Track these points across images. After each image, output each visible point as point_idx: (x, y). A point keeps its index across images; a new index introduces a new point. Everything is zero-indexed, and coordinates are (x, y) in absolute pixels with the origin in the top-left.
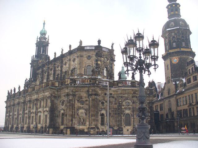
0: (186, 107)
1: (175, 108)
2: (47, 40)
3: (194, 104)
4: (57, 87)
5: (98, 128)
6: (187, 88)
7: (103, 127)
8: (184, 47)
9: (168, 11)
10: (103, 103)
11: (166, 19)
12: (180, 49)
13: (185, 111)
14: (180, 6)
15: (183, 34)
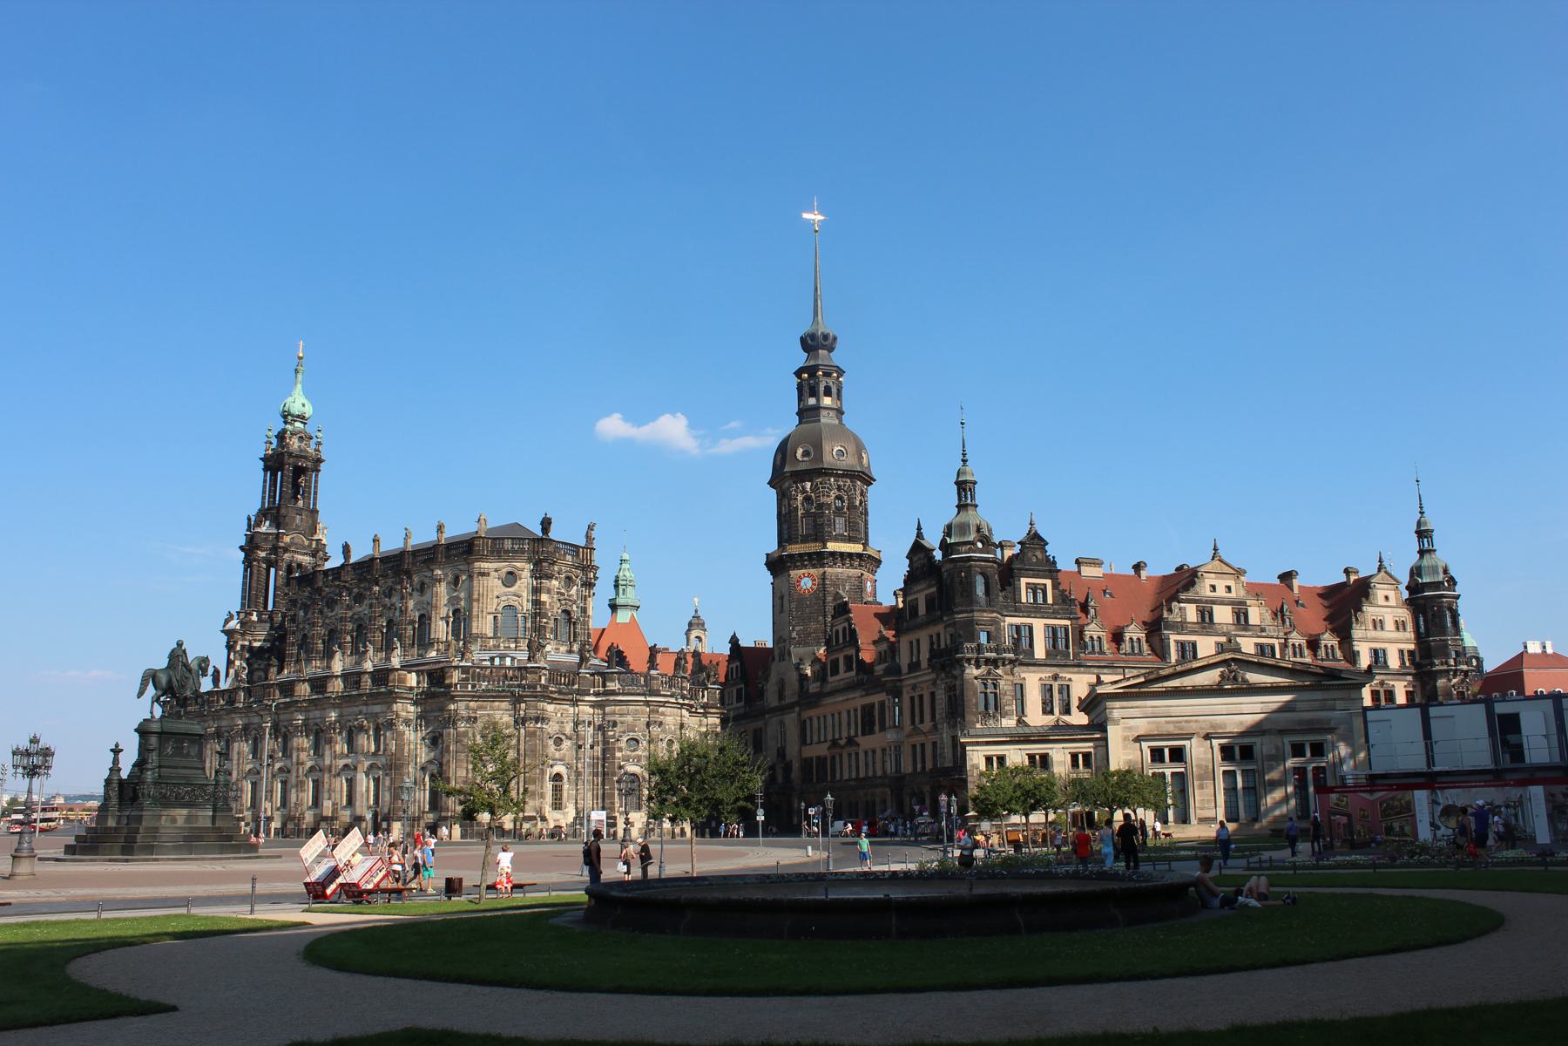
0: (821, 750)
1: (796, 748)
2: (313, 446)
3: (842, 742)
4: (411, 688)
5: (544, 819)
6: (828, 688)
7: (557, 815)
8: (837, 539)
9: (800, 388)
10: (558, 742)
11: (788, 424)
12: (825, 546)
13: (821, 761)
14: (841, 372)
15: (839, 488)
